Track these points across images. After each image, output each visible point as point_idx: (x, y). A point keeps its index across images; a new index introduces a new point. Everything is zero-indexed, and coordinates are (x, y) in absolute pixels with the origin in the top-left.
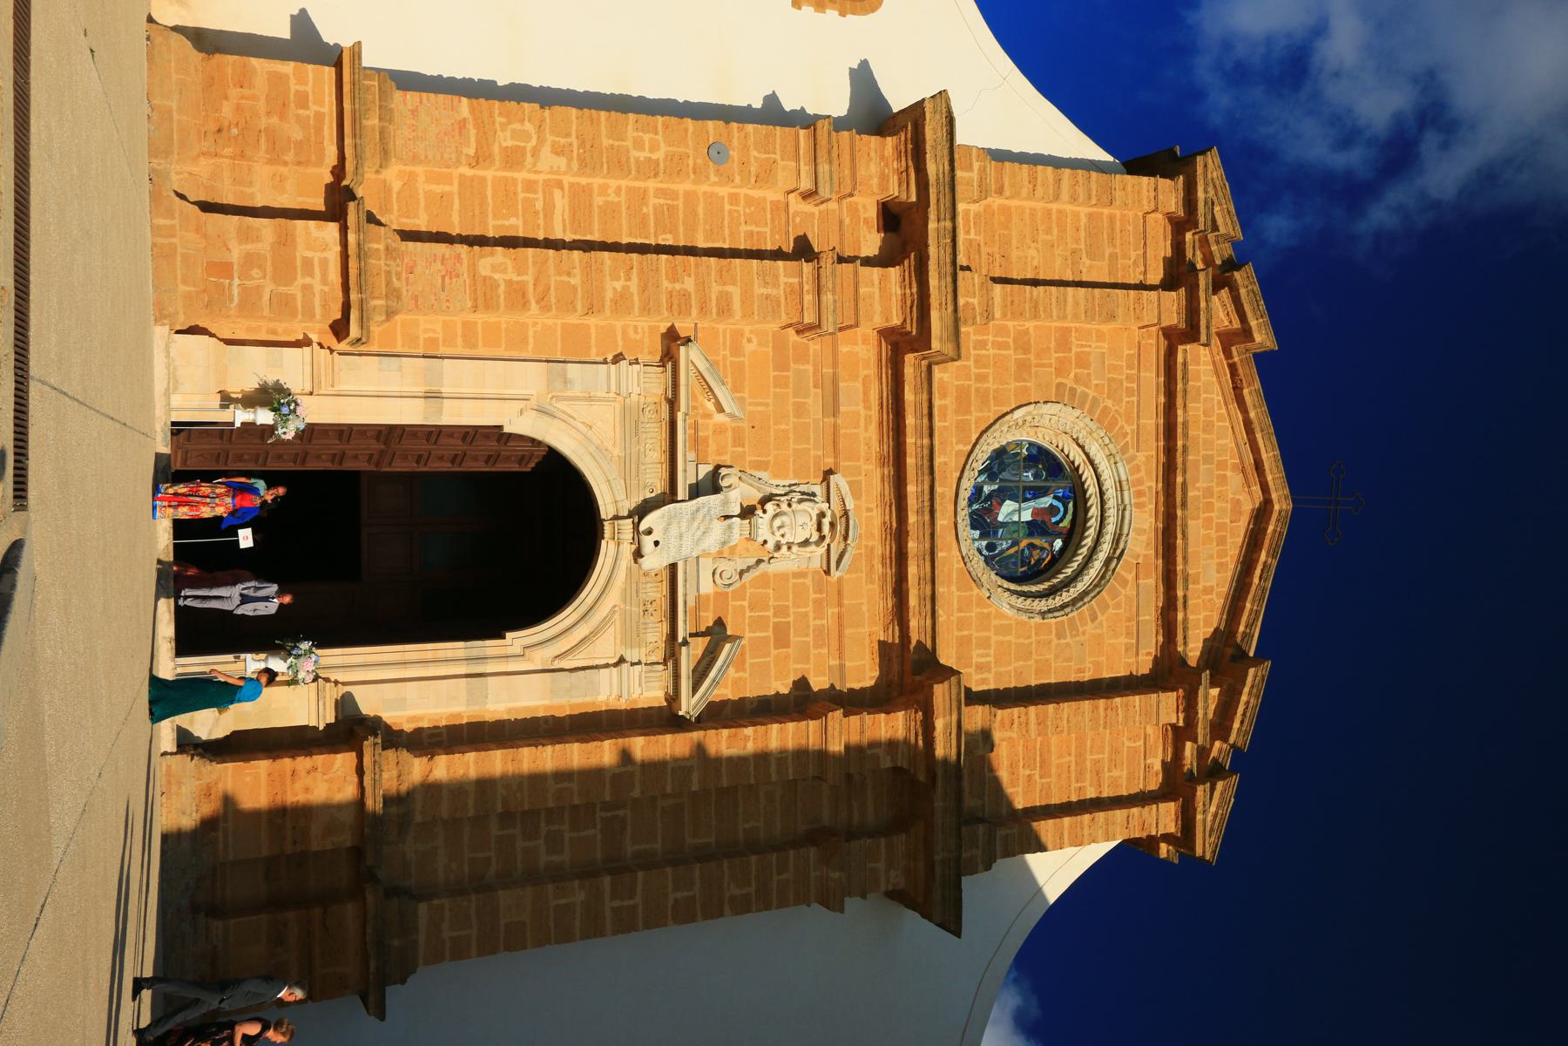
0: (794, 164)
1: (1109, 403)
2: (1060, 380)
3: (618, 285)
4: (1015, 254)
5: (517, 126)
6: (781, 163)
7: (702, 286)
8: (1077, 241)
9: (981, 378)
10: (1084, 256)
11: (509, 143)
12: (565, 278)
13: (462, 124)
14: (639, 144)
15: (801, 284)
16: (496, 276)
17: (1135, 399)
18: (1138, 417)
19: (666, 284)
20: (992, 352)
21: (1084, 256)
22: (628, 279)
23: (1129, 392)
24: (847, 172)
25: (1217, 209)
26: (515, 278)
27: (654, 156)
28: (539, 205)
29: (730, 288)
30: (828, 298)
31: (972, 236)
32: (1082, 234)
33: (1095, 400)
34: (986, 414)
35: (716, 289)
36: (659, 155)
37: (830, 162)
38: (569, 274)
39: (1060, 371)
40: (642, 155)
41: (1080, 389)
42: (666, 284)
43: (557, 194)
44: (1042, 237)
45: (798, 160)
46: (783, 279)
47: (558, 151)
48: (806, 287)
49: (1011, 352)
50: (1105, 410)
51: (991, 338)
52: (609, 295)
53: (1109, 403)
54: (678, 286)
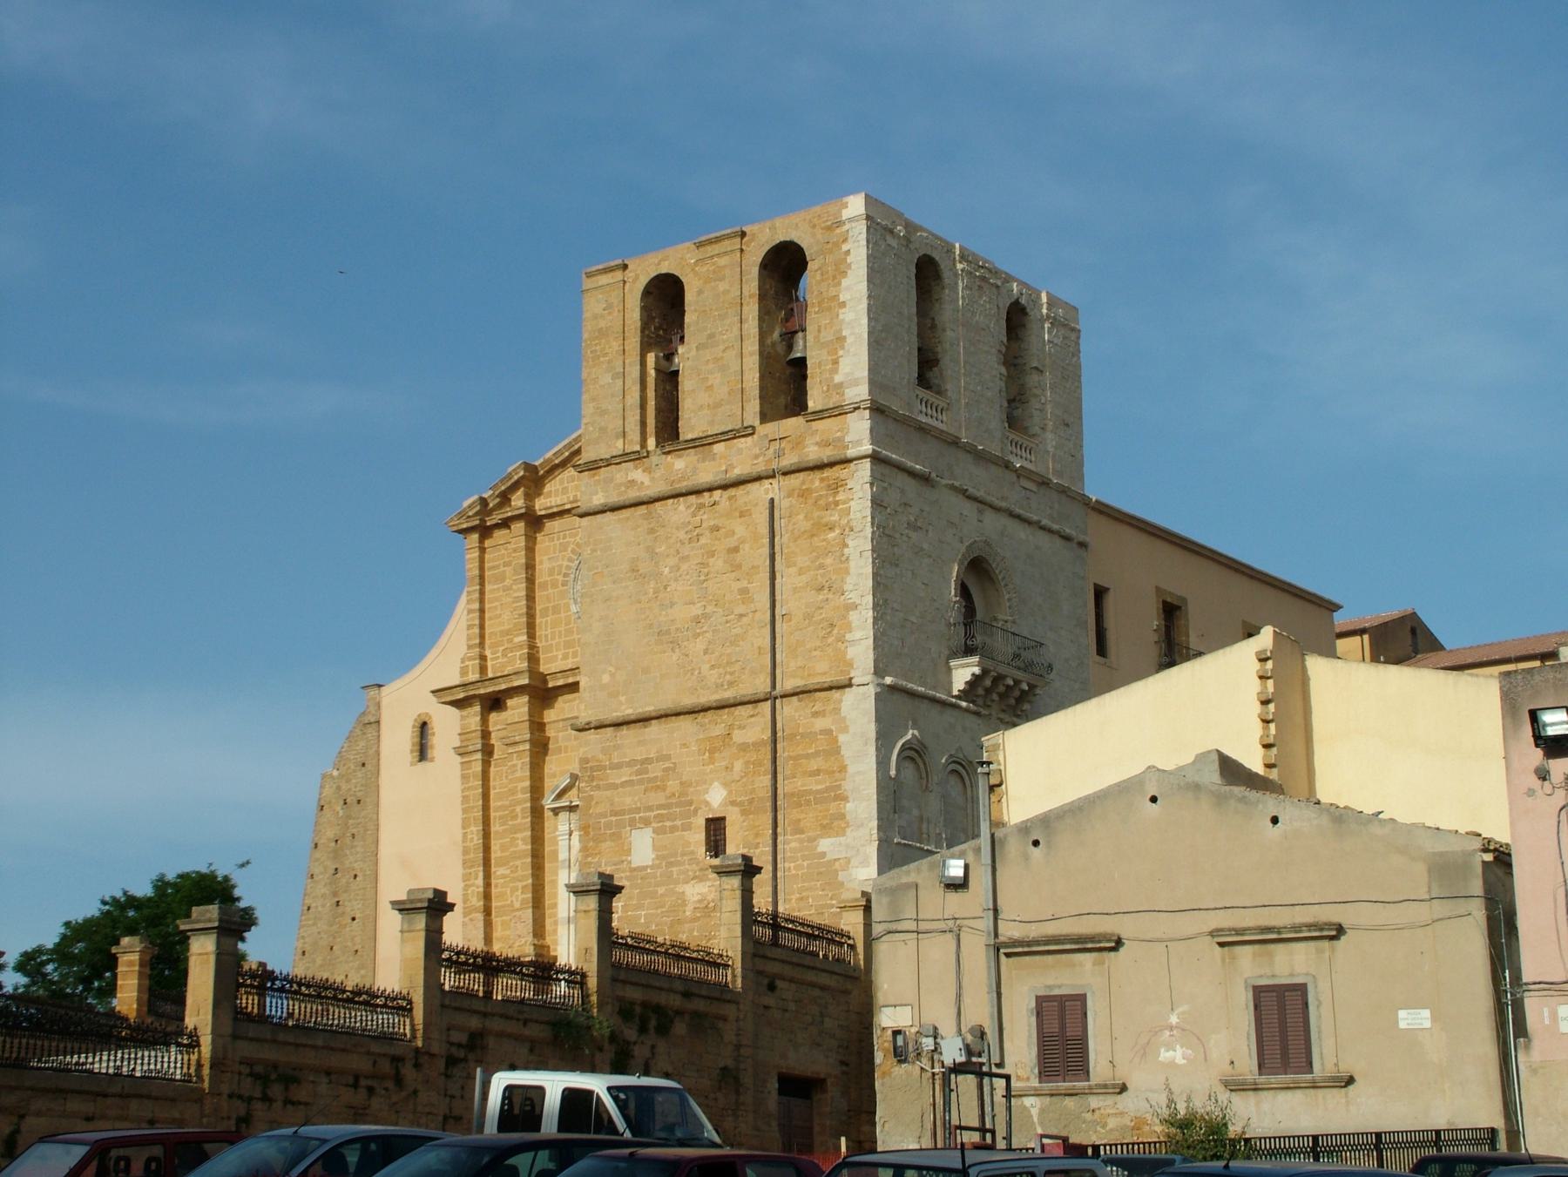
0: (473, 763)
1: (570, 549)
2: (560, 585)
3: (520, 842)
4: (506, 627)
5: (470, 897)
6: (473, 770)
7: (519, 802)
8: (498, 589)
9: (560, 637)
10: (506, 583)
11: (475, 899)
12: (519, 868)
13: (471, 920)
14: (472, 839)
15: (515, 752)
16: (520, 899)
17: (567, 532)
18: (575, 529)
19: (519, 820)
20: (549, 631)
21: (506, 583)
22: (518, 839)
23: (564, 538)
24: (474, 734)
25: (470, 514)
26: (520, 891)
27: (475, 833)
28: (502, 881)
29: (519, 788)
30: (517, 739)
31: (499, 654)
32: (495, 587)
33: (570, 560)
34: (575, 629)
35: (520, 796)
36: (473, 829)
37: (468, 746)
38: (517, 867)
39: (557, 587)
40: (476, 838)
41: (564, 571)
42: (519, 820)
43: (498, 873)
44: (498, 612)
45: (470, 761)
46: (514, 762)
47: (476, 878)
48: (517, 750)
49: (548, 618)
50: (573, 551)
51: (543, 633)
52: (524, 847)
53: (570, 549)
54: (520, 815)
